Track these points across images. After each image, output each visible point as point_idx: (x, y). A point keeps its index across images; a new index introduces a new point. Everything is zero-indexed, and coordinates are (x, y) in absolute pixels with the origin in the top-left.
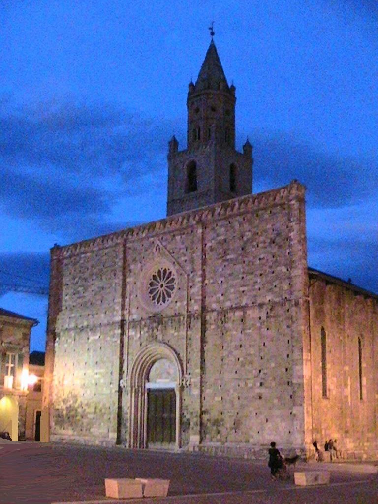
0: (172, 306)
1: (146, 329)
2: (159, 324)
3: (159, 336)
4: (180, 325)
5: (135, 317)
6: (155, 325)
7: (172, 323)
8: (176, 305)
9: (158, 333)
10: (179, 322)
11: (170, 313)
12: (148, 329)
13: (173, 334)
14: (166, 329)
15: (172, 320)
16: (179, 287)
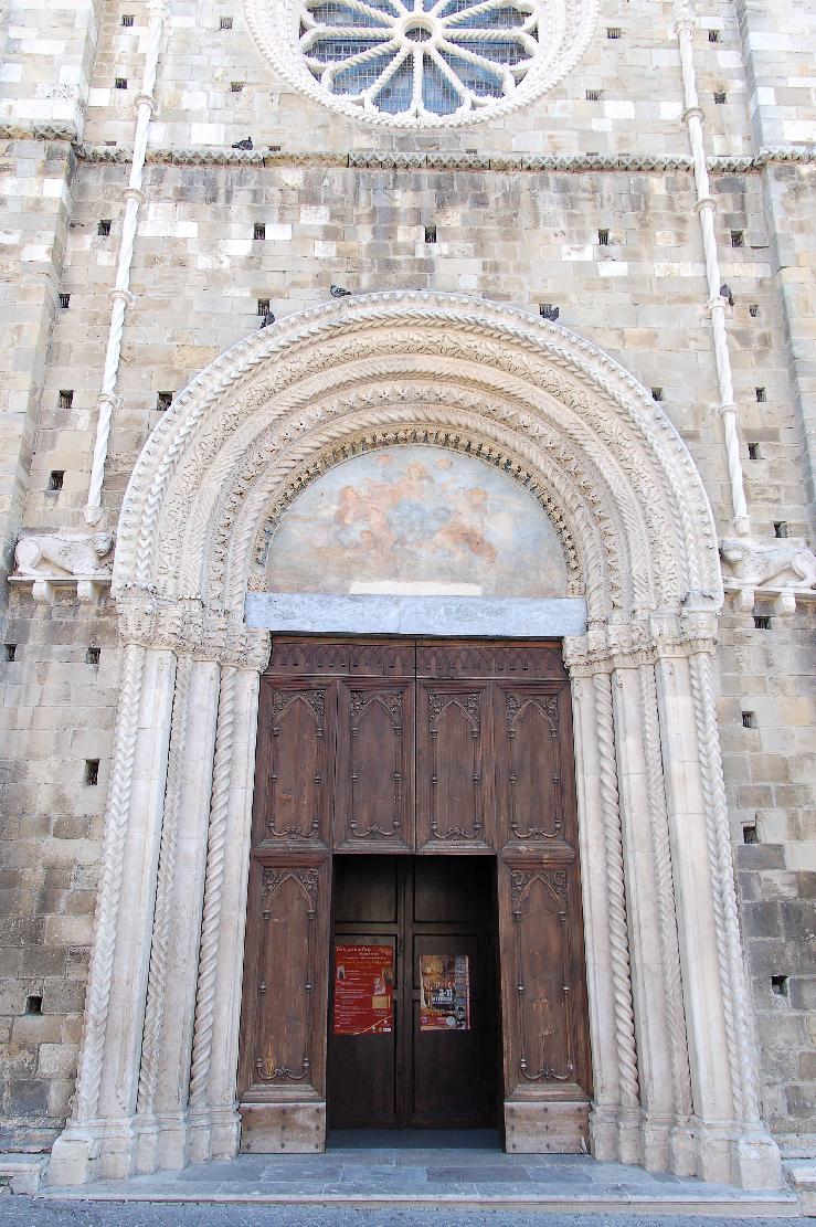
0: (557, 110)
1: (317, 217)
2: (441, 205)
3: (442, 268)
4: (644, 224)
5: (208, 136)
6: (403, 200)
7: (570, 202)
8: (601, 115)
9: (440, 248)
10: (640, 201)
11: (535, 146)
12: (333, 216)
13: (579, 265)
14: (509, 235)
15: (564, 188)
16: (614, 24)
